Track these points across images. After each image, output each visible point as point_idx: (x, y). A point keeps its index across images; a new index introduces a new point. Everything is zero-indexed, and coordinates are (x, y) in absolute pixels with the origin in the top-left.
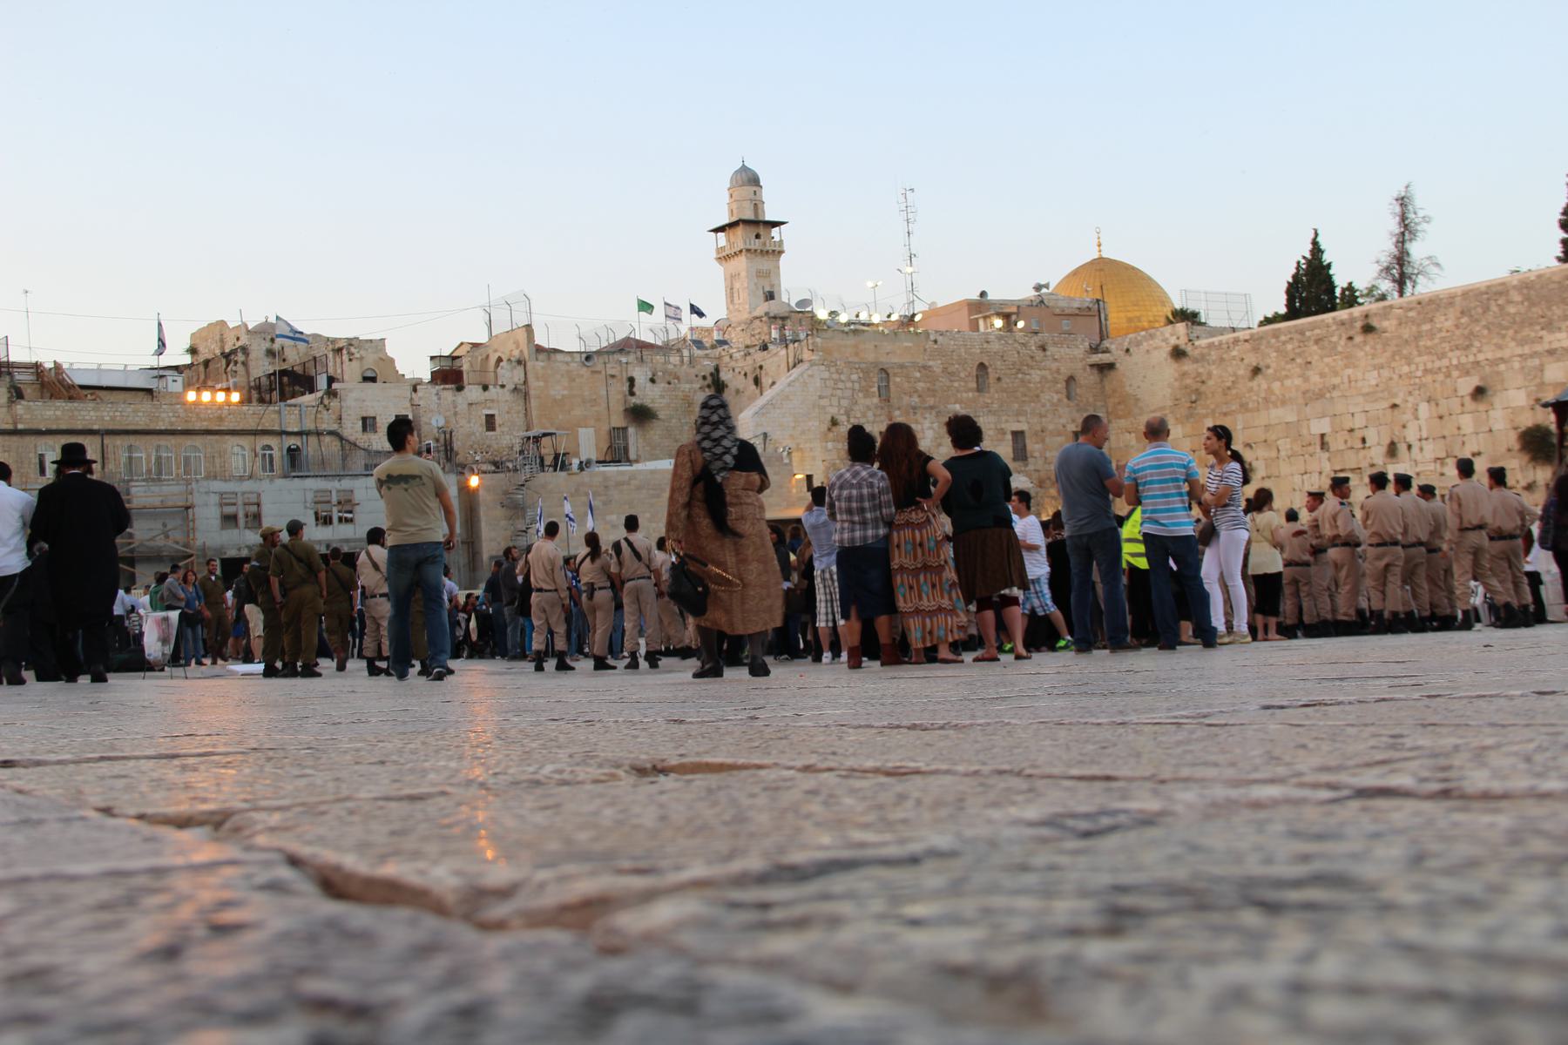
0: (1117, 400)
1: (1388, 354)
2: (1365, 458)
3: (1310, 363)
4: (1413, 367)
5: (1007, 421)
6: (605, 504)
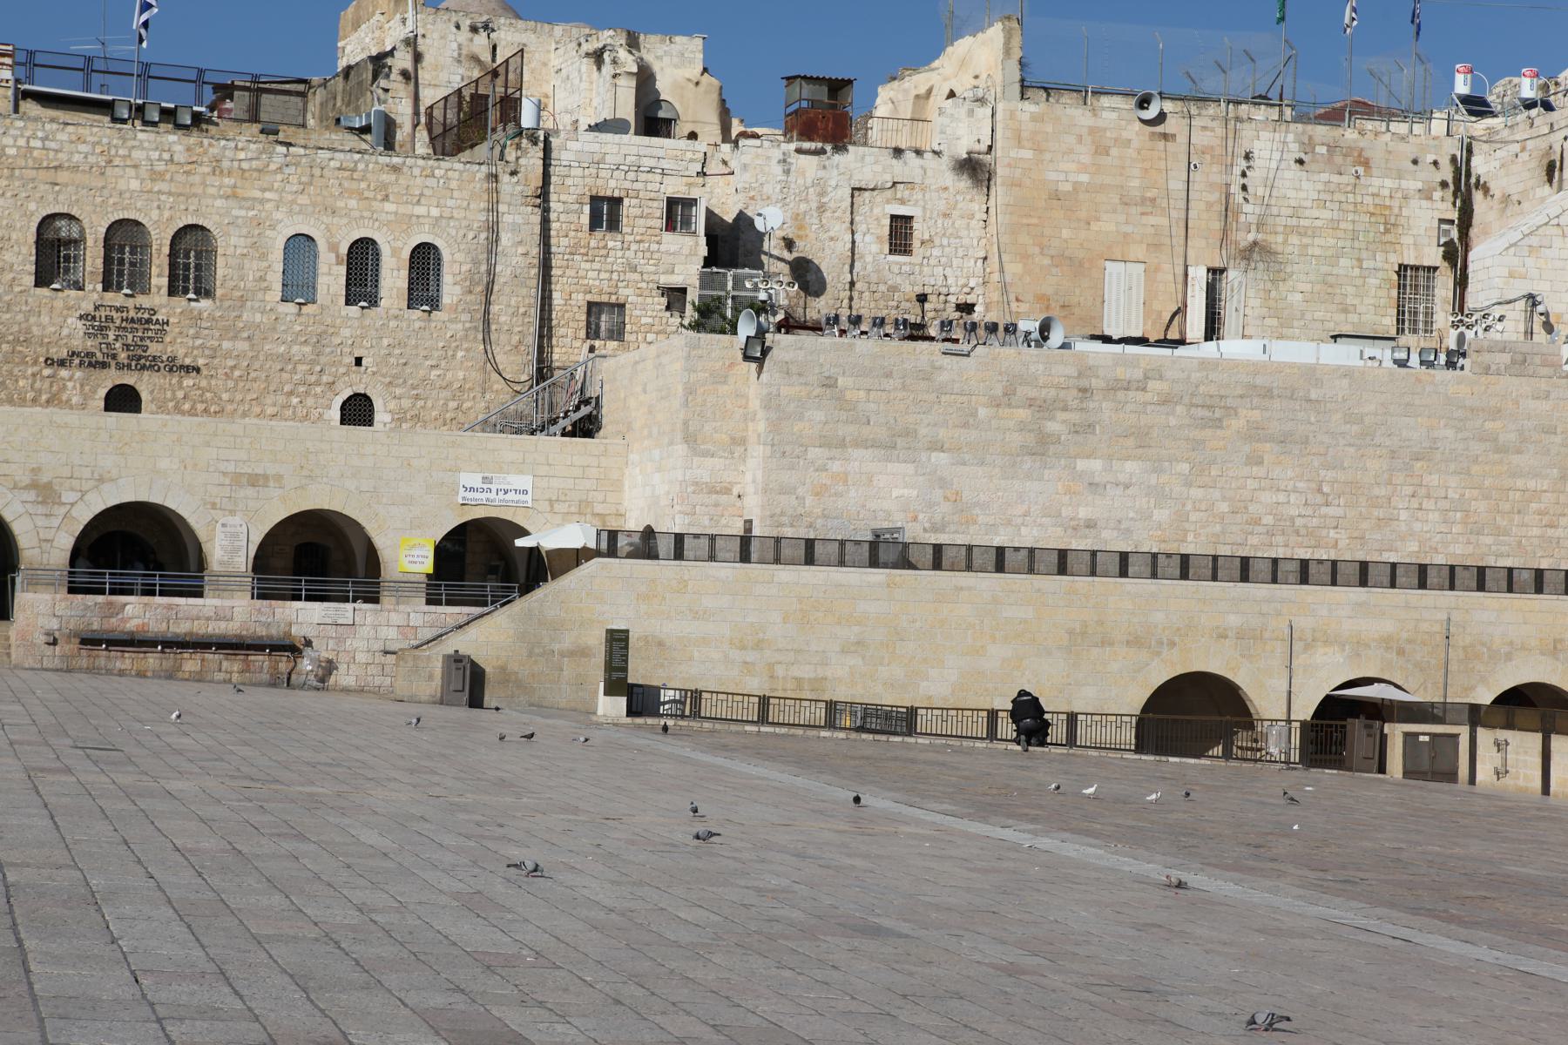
6: (1076, 430)
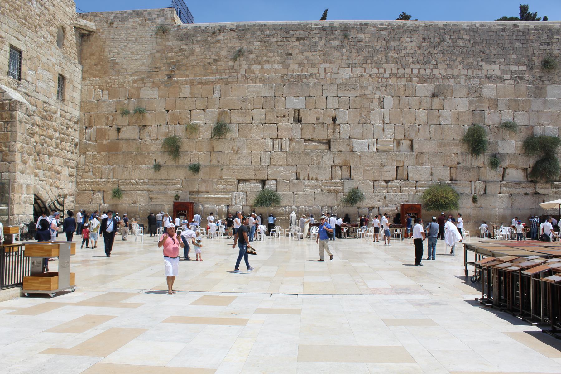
0: (93, 62)
1: (361, 58)
3: (291, 54)
4: (381, 70)
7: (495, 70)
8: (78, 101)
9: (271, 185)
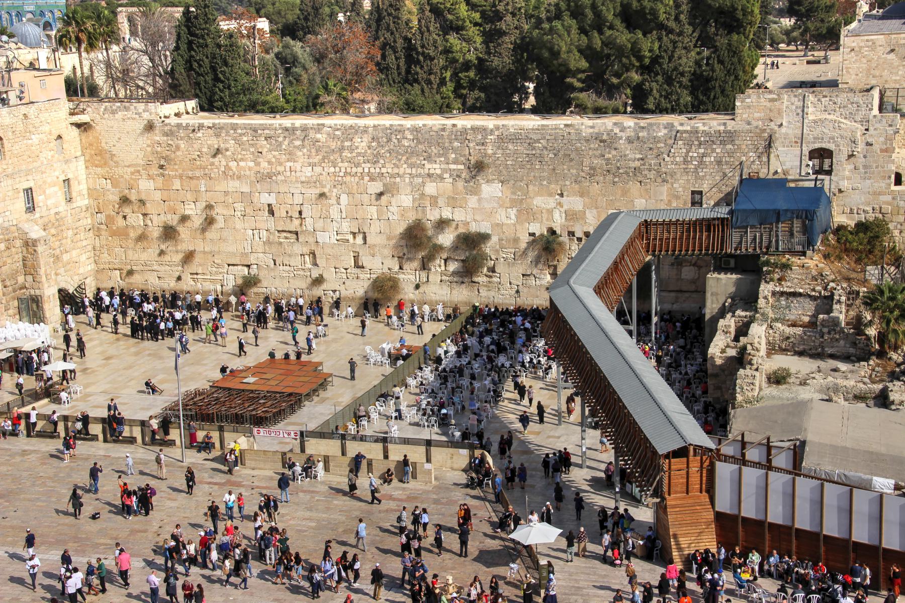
0: (93, 152)
2: (301, 225)
4: (337, 169)
5: (20, 182)
7: (435, 168)
8: (85, 192)
9: (254, 270)
